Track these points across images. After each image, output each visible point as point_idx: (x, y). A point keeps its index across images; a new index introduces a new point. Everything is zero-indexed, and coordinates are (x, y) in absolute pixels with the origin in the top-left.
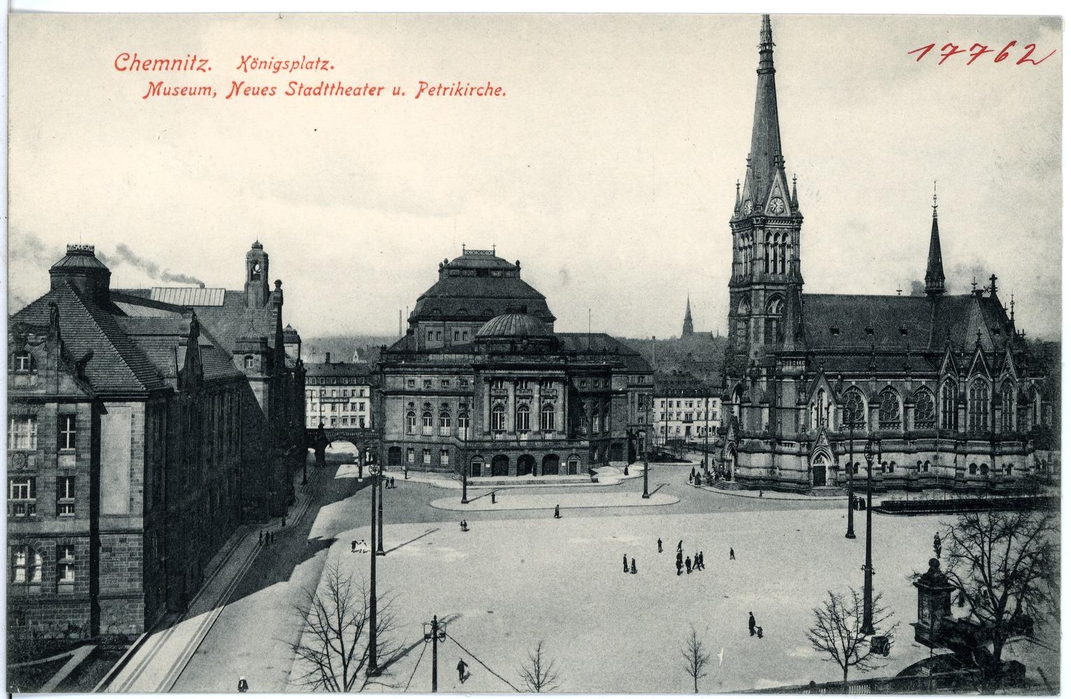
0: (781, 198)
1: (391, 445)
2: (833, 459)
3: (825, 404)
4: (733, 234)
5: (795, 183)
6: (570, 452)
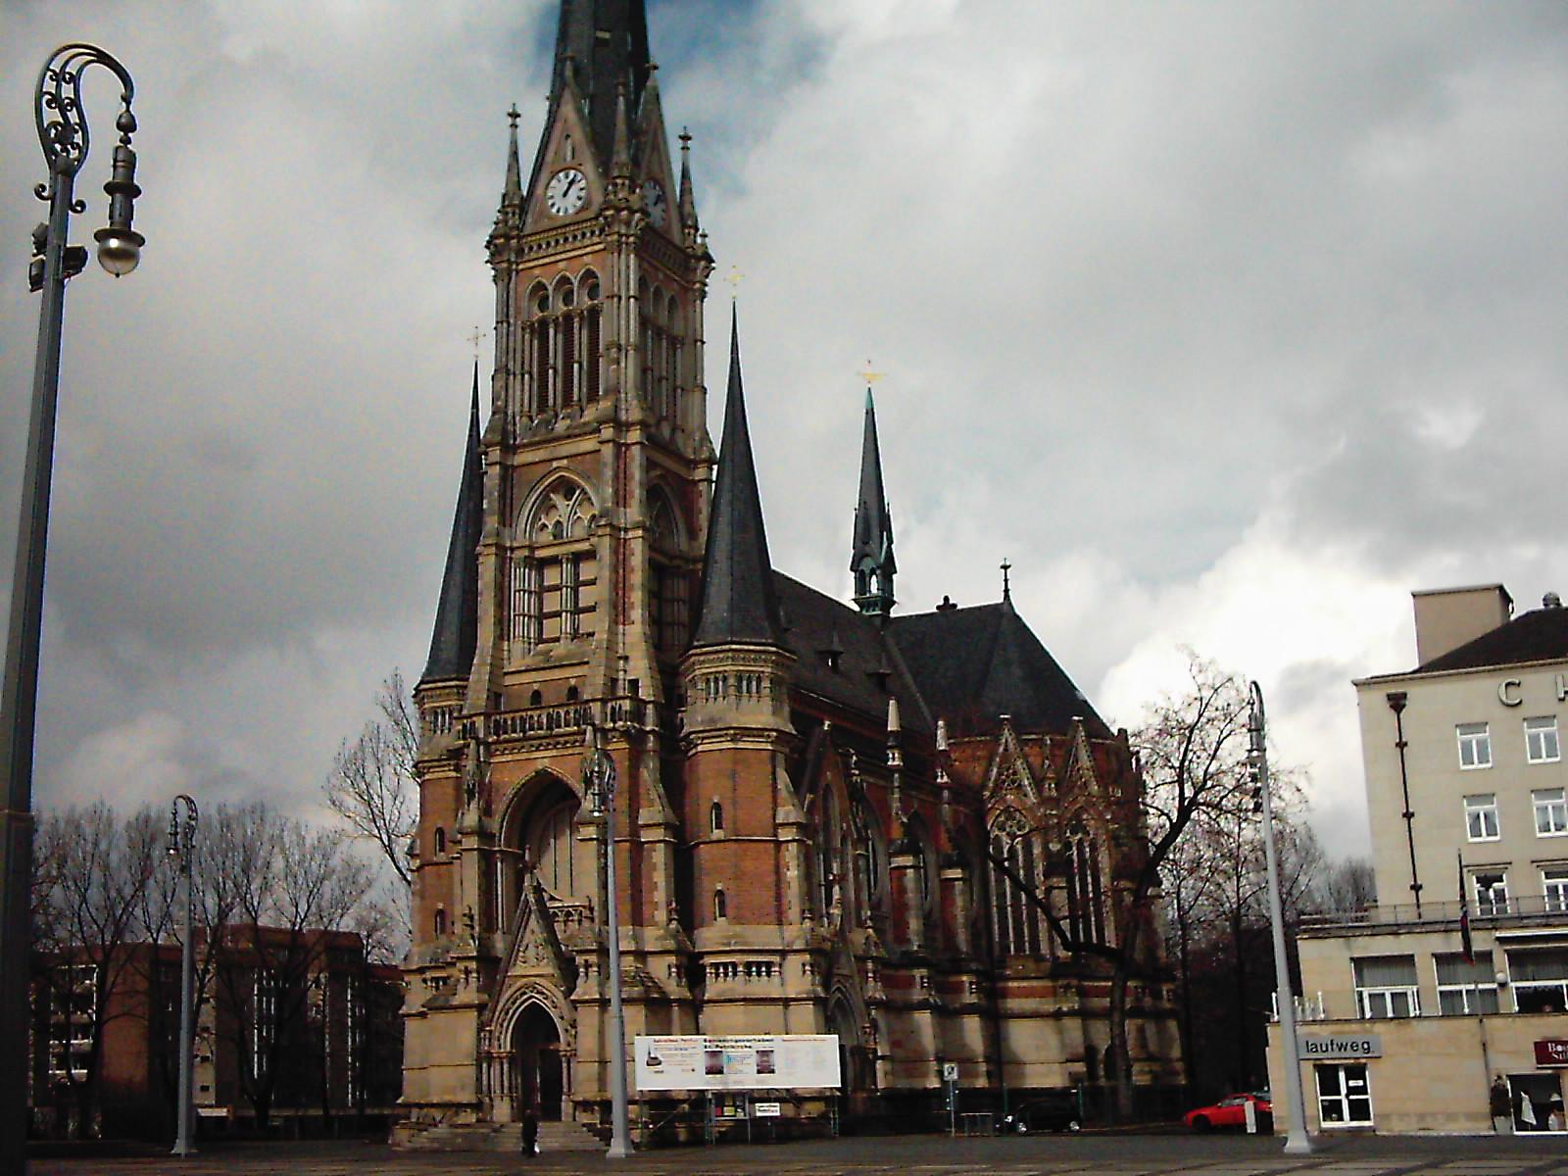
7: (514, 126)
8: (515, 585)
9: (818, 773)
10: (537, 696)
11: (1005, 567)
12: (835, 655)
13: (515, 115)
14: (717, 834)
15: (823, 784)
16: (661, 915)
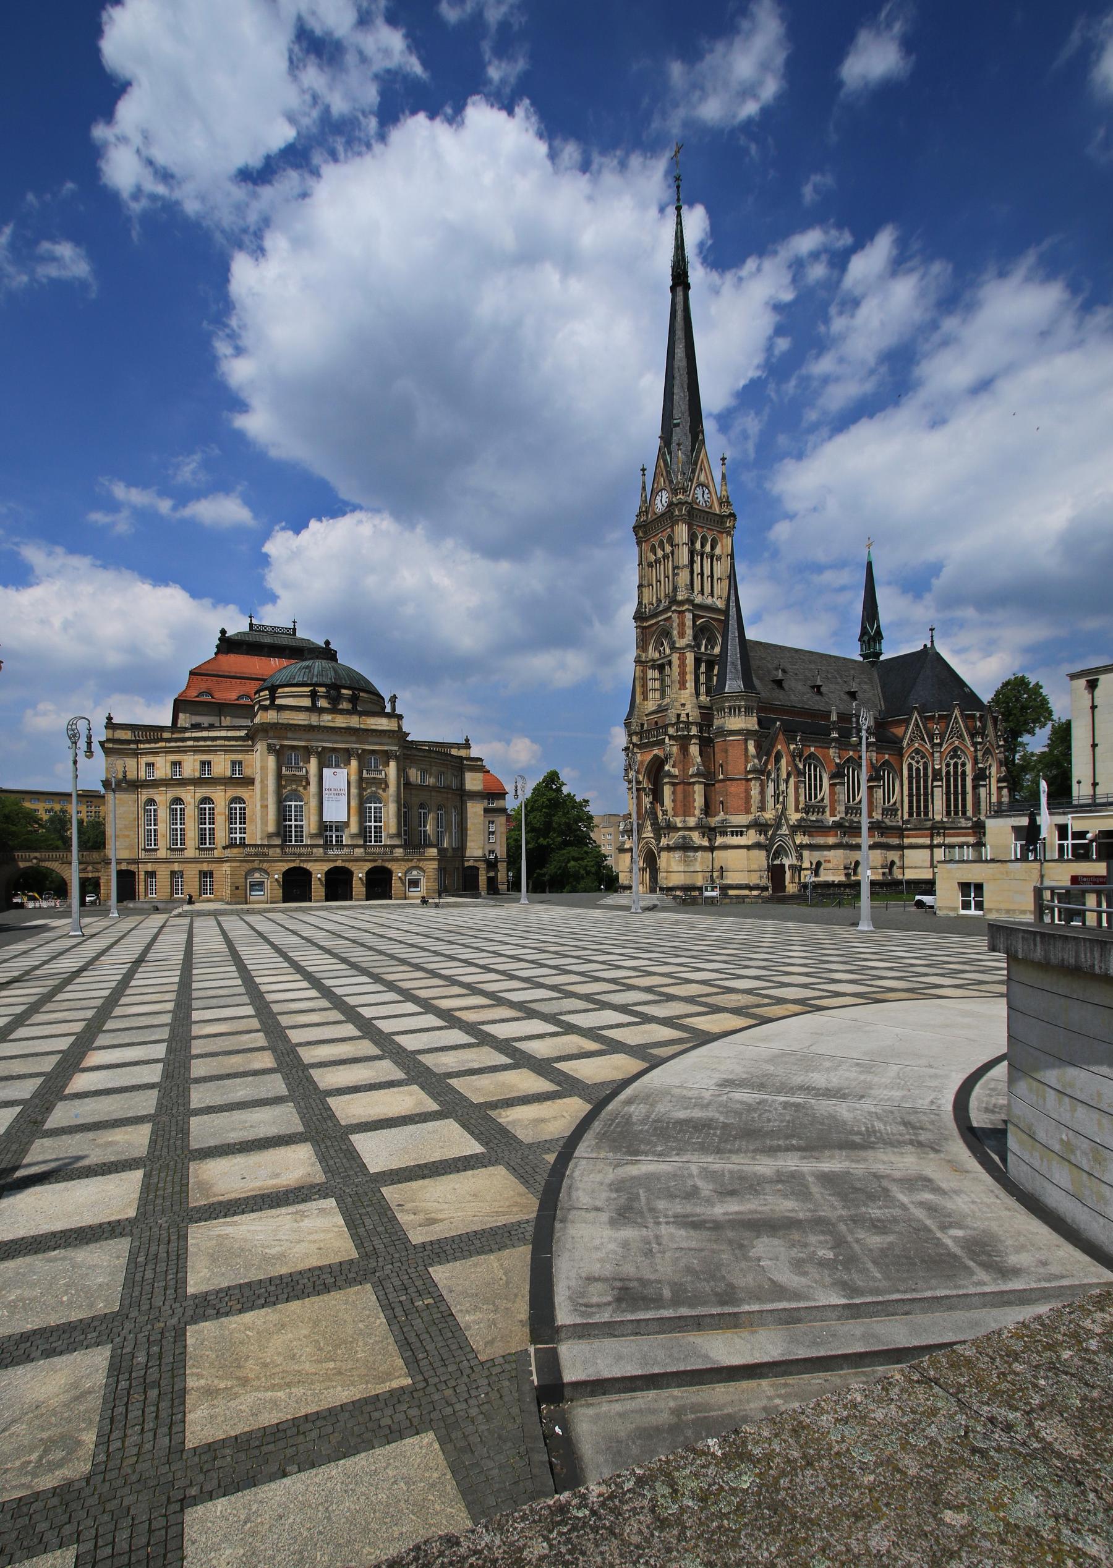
2: (794, 854)
3: (784, 776)
4: (639, 543)
8: (649, 677)
9: (773, 746)
10: (656, 723)
11: (932, 630)
12: (819, 687)
13: (643, 470)
14: (721, 777)
15: (775, 751)
16: (697, 812)
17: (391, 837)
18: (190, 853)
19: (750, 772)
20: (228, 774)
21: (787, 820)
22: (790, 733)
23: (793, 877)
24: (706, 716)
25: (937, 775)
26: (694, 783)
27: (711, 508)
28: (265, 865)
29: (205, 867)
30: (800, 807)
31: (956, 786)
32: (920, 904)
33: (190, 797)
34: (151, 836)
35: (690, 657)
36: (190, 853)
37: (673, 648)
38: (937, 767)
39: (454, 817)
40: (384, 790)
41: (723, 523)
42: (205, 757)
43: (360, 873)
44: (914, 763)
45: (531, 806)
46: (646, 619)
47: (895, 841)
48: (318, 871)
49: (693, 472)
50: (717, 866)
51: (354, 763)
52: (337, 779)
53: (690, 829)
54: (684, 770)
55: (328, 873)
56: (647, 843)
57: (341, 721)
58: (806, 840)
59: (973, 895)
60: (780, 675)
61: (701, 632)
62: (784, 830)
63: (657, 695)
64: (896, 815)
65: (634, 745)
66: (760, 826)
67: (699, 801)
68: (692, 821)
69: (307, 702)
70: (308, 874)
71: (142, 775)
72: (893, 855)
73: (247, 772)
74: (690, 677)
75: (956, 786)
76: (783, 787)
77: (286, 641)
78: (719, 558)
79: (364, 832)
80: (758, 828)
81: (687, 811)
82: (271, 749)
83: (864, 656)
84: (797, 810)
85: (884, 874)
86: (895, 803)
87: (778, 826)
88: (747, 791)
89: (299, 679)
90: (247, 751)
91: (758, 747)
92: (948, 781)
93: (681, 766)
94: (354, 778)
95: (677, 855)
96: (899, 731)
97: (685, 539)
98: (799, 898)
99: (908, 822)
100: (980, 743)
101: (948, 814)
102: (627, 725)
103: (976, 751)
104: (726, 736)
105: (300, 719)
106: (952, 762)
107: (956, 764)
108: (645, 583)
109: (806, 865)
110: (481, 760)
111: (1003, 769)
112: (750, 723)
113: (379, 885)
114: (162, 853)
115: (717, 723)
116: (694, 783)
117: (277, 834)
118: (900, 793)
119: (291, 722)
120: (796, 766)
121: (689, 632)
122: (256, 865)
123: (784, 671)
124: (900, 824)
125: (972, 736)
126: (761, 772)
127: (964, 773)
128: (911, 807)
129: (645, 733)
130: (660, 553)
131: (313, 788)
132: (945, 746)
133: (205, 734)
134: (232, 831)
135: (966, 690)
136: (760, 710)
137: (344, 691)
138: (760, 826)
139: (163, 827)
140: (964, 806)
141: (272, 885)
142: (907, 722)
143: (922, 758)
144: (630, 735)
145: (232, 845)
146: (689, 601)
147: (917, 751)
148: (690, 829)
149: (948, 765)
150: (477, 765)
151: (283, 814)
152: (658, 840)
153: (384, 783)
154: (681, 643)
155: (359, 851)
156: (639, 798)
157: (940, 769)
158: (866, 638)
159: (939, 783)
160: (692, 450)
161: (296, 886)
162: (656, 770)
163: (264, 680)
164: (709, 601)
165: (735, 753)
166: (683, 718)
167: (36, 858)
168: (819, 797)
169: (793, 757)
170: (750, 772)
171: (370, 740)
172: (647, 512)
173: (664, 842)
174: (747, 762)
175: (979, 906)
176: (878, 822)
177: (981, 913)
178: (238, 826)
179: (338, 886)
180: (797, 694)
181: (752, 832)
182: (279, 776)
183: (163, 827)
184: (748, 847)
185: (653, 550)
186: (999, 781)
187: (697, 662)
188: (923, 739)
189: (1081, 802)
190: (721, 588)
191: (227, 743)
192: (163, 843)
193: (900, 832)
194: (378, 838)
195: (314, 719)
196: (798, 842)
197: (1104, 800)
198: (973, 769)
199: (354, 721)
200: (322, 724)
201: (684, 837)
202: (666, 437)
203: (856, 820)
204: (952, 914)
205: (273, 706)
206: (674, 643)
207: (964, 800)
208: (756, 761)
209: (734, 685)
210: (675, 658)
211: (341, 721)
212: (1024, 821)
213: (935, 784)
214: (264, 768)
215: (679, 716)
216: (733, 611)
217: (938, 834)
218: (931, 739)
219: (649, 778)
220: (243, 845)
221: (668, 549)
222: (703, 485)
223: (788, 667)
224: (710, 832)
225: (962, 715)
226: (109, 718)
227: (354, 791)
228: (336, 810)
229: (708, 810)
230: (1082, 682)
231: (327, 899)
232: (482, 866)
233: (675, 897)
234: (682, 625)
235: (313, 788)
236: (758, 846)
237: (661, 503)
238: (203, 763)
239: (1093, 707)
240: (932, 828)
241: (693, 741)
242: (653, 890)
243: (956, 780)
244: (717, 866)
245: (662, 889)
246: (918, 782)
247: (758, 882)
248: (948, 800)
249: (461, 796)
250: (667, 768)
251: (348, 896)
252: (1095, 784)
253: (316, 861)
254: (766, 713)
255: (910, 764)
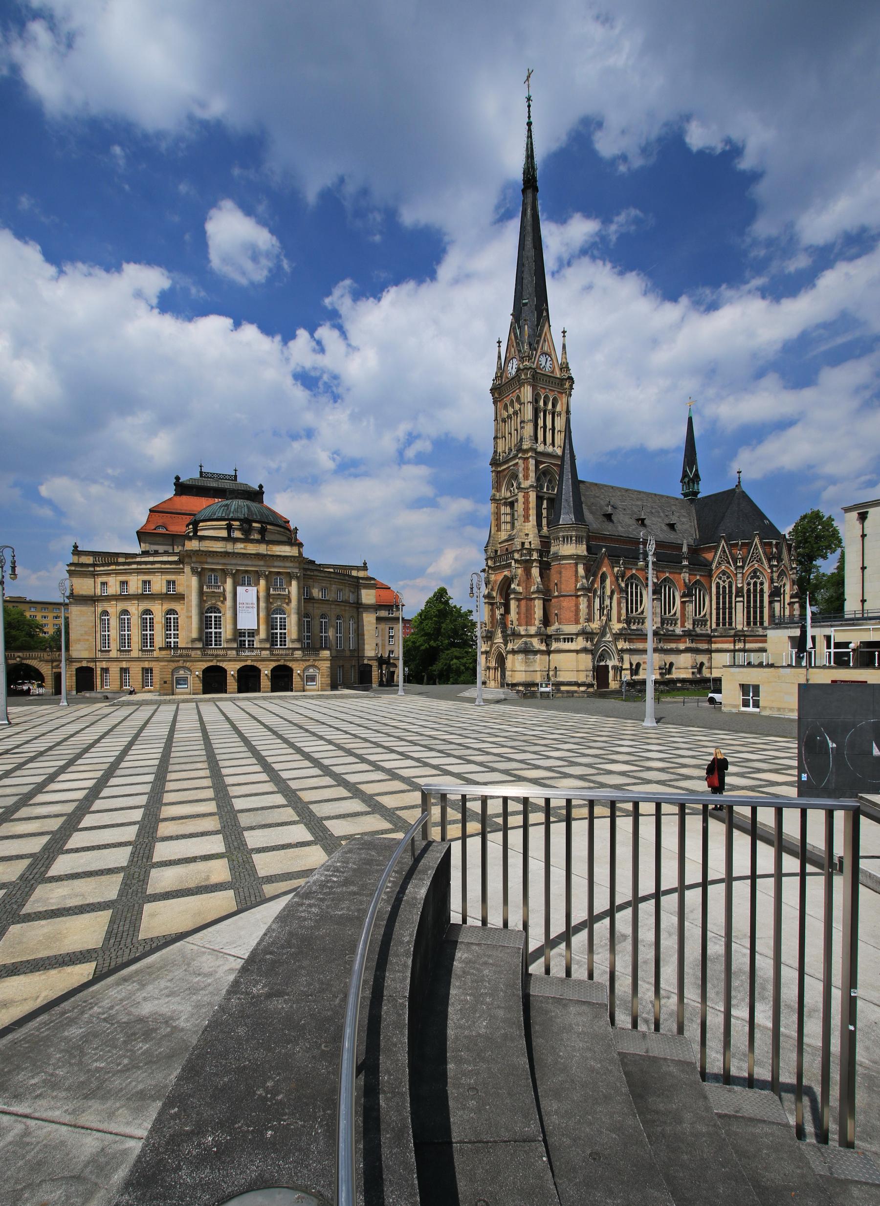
0: (550, 356)
1: (78, 665)
2: (616, 657)
3: (608, 593)
4: (495, 403)
5: (564, 336)
6: (308, 663)
7: (499, 346)
8: (502, 512)
9: (599, 567)
11: (739, 472)
12: (643, 520)
14: (556, 594)
16: (537, 622)
17: (293, 641)
18: (135, 654)
19: (579, 590)
20: (164, 591)
21: (610, 629)
22: (614, 557)
23: (615, 676)
24: (545, 544)
25: (739, 592)
26: (534, 599)
27: (552, 372)
28: (188, 664)
29: (146, 665)
30: (622, 618)
31: (755, 601)
32: (712, 701)
33: (135, 609)
34: (105, 640)
35: (533, 496)
36: (135, 654)
37: (519, 488)
38: (739, 585)
39: (352, 625)
40: (288, 604)
41: (562, 385)
42: (146, 578)
43: (266, 670)
44: (721, 583)
45: (424, 616)
46: (500, 465)
47: (704, 646)
48: (232, 669)
49: (538, 342)
50: (552, 667)
51: (262, 582)
52: (248, 595)
53: (531, 636)
54: (527, 588)
55: (240, 671)
56: (498, 647)
57: (252, 549)
58: (627, 646)
59: (751, 695)
60: (609, 510)
61: (542, 475)
62: (608, 637)
63: (509, 526)
64: (705, 625)
65: (489, 567)
66: (587, 635)
67: (538, 613)
68: (533, 630)
69: (224, 533)
70: (223, 671)
71: (98, 592)
72: (703, 658)
73: (180, 589)
74: (533, 513)
75: (755, 601)
76: (607, 602)
77: (226, 485)
78: (560, 414)
79: (272, 639)
80: (585, 636)
81: (529, 623)
82: (194, 571)
83: (685, 495)
84: (619, 621)
85: (693, 673)
86: (705, 615)
87: (603, 634)
88: (577, 606)
89: (219, 515)
90: (180, 572)
91: (587, 570)
92: (749, 597)
93: (524, 585)
94: (262, 594)
95: (520, 657)
96: (709, 556)
97: (530, 398)
98: (617, 693)
99: (715, 630)
100: (776, 566)
101: (748, 624)
102: (486, 551)
103: (772, 572)
104: (560, 560)
105: (218, 547)
106: (752, 581)
107: (755, 584)
108: (499, 435)
109: (626, 665)
110: (373, 579)
111: (796, 587)
112: (582, 550)
113: (282, 679)
114: (114, 654)
115: (553, 549)
116: (534, 599)
117: (199, 639)
118: (710, 606)
119: (211, 549)
120: (619, 585)
121: (532, 475)
122: (180, 664)
123: (614, 507)
124: (709, 632)
125: (769, 560)
126: (588, 590)
127: (762, 590)
128: (718, 619)
129: (498, 558)
130: (511, 411)
131: (229, 602)
132: (746, 568)
133: (151, 559)
134: (168, 636)
135: (766, 522)
136: (589, 539)
137: (254, 525)
138: (587, 635)
139: (114, 633)
140: (762, 617)
141: (194, 680)
142: (716, 548)
143: (728, 578)
144: (487, 560)
145: (168, 647)
146: (531, 449)
147: (724, 573)
148: (531, 636)
149: (749, 584)
150: (371, 583)
151: (205, 623)
152: (506, 645)
153: (288, 597)
154: (525, 484)
155: (266, 653)
156: (492, 610)
157: (742, 587)
158: (686, 480)
159: (741, 599)
160: (537, 325)
161: (213, 681)
162: (505, 587)
163: (194, 515)
164: (550, 449)
165: (567, 574)
166: (527, 546)
167: (19, 657)
168: (639, 611)
169: (617, 578)
170: (579, 590)
171: (276, 564)
172: (501, 377)
173: (510, 646)
174: (577, 581)
175: (756, 704)
176: (689, 631)
177: (757, 710)
178: (172, 632)
179: (248, 680)
180: (624, 525)
181: (580, 639)
182: (201, 593)
183: (114, 633)
184: (577, 652)
185: (506, 408)
186: (792, 597)
187: (540, 499)
188: (729, 563)
189: (870, 615)
190: (559, 439)
191: (163, 566)
192: (114, 646)
193: (709, 639)
194: (283, 642)
195: (230, 547)
196: (619, 647)
197: (853, 616)
198: (770, 586)
199: (262, 549)
200: (236, 551)
201: (526, 643)
202: (517, 315)
203: (671, 628)
204: (734, 710)
205: (196, 536)
206: (519, 484)
207: (762, 612)
208: (584, 581)
209: (567, 518)
210: (520, 496)
211: (252, 549)
212: (797, 632)
213: (738, 599)
214: (189, 586)
215: (523, 544)
216: (567, 457)
217: (739, 641)
218: (735, 563)
219: (501, 595)
220: (176, 648)
221: (517, 406)
222: (546, 354)
223: (618, 504)
224: (547, 639)
225: (761, 542)
226: (76, 547)
227: (262, 605)
228: (248, 620)
229: (546, 622)
230: (854, 515)
231: (273, 691)
232: (375, 664)
233: (518, 692)
234: (526, 469)
235: (229, 602)
236: (585, 650)
237: (512, 369)
238: (145, 582)
239: (863, 536)
240: (735, 636)
241: (535, 564)
242: (502, 686)
243: (755, 596)
244: (552, 667)
245: (508, 685)
246: (724, 598)
247: (584, 680)
248: (749, 612)
249: (358, 608)
250: (513, 586)
251: (256, 688)
252: (863, 601)
253: (230, 661)
254: (593, 541)
255: (718, 583)
